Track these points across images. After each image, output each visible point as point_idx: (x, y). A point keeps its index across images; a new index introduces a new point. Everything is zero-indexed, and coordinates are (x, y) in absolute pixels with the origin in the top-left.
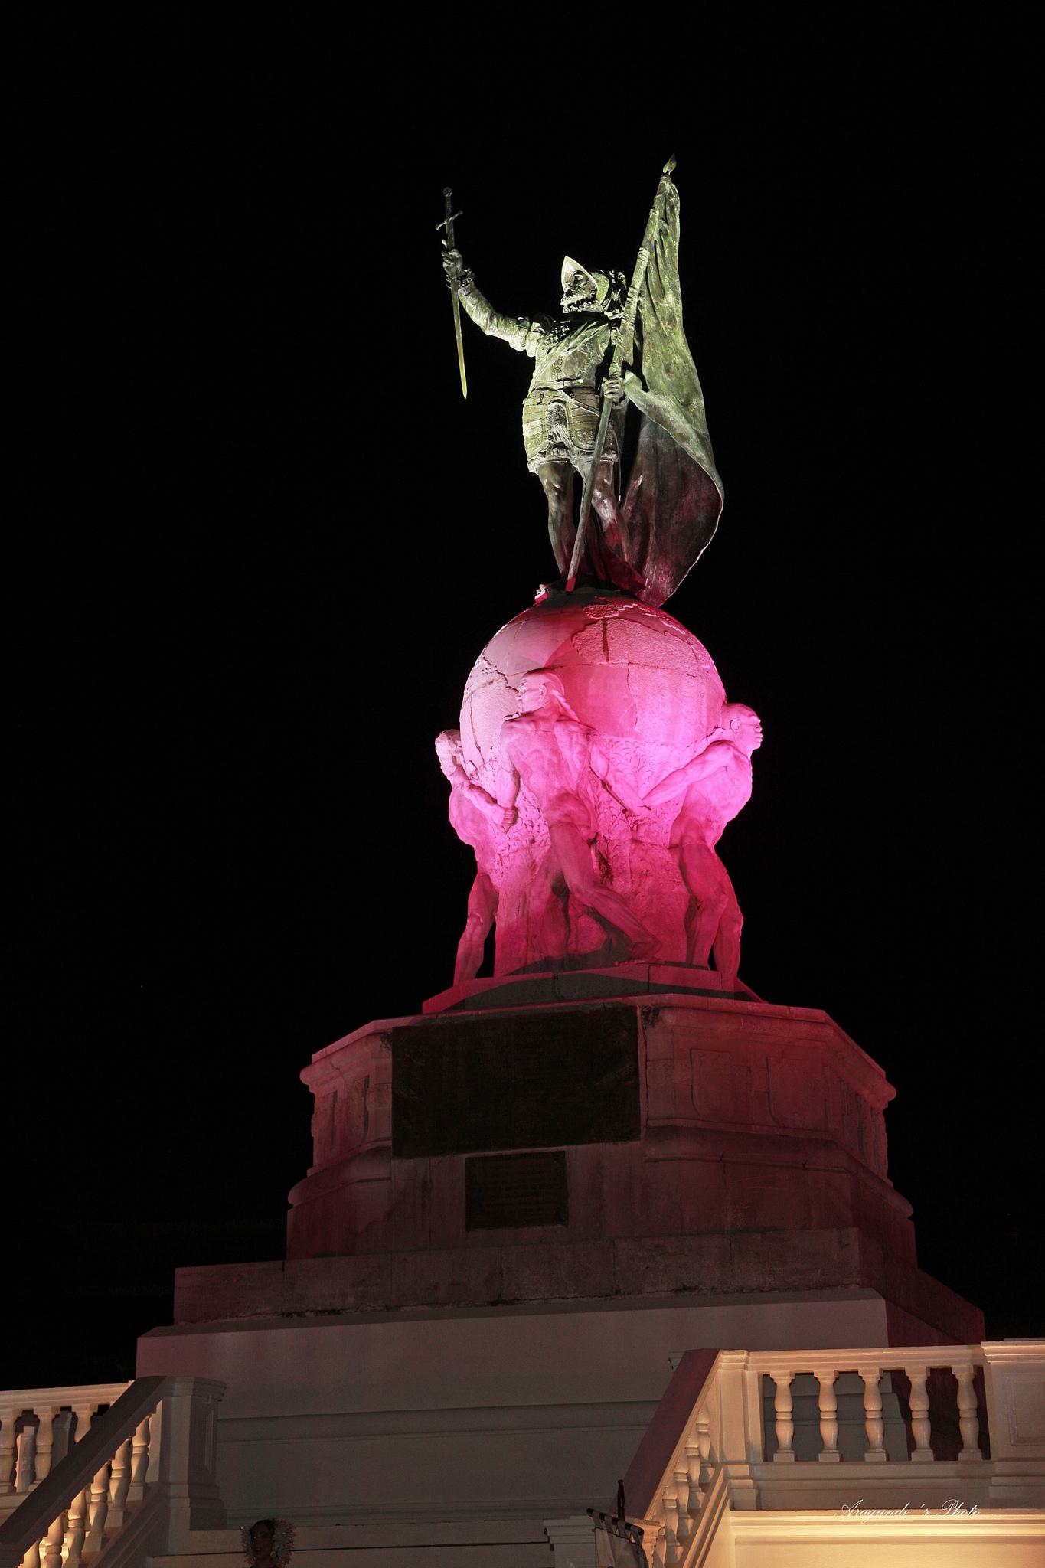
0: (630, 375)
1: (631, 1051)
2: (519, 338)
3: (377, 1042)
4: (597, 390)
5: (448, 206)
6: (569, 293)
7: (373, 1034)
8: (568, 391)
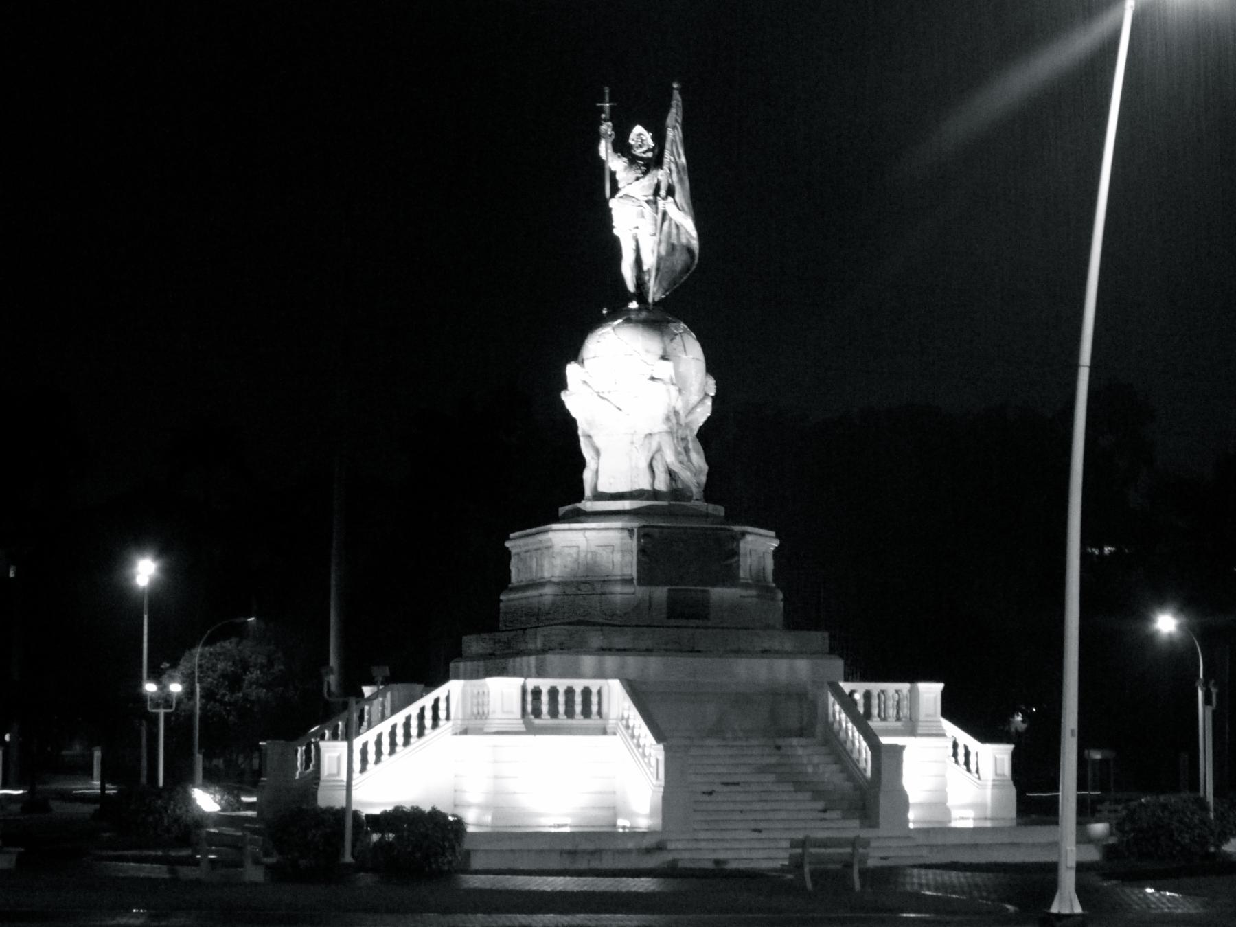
0: (670, 199)
1: (735, 553)
2: (616, 164)
3: (626, 534)
4: (655, 202)
5: (607, 98)
6: (641, 146)
7: (622, 529)
8: (647, 202)
